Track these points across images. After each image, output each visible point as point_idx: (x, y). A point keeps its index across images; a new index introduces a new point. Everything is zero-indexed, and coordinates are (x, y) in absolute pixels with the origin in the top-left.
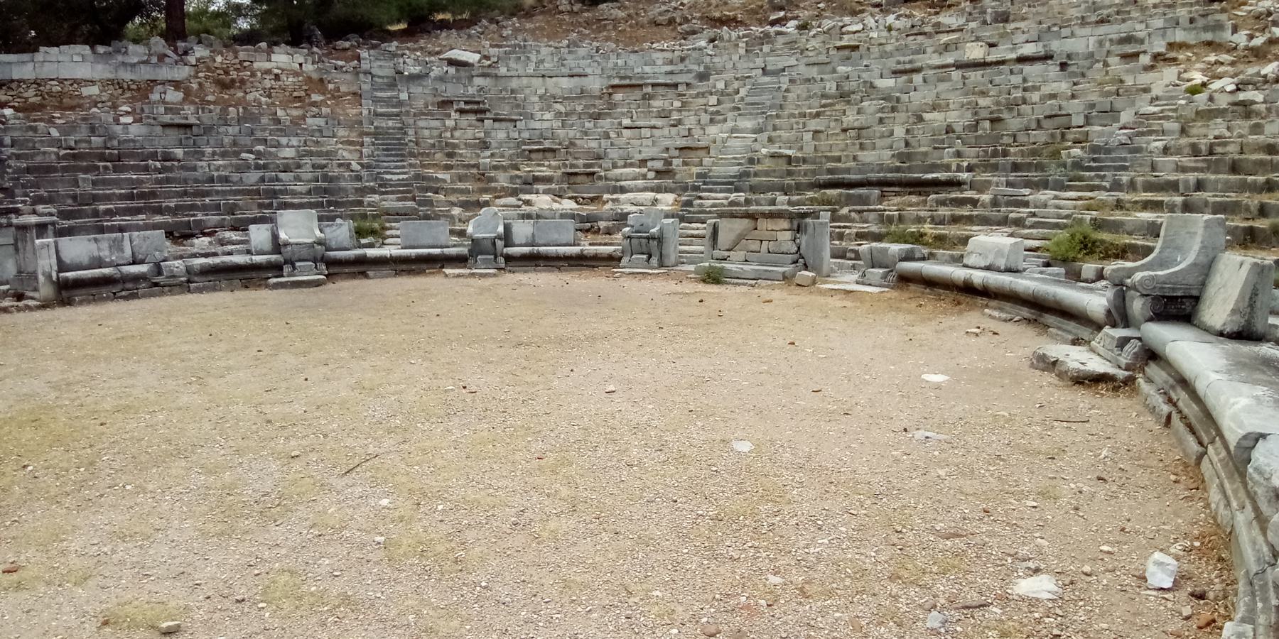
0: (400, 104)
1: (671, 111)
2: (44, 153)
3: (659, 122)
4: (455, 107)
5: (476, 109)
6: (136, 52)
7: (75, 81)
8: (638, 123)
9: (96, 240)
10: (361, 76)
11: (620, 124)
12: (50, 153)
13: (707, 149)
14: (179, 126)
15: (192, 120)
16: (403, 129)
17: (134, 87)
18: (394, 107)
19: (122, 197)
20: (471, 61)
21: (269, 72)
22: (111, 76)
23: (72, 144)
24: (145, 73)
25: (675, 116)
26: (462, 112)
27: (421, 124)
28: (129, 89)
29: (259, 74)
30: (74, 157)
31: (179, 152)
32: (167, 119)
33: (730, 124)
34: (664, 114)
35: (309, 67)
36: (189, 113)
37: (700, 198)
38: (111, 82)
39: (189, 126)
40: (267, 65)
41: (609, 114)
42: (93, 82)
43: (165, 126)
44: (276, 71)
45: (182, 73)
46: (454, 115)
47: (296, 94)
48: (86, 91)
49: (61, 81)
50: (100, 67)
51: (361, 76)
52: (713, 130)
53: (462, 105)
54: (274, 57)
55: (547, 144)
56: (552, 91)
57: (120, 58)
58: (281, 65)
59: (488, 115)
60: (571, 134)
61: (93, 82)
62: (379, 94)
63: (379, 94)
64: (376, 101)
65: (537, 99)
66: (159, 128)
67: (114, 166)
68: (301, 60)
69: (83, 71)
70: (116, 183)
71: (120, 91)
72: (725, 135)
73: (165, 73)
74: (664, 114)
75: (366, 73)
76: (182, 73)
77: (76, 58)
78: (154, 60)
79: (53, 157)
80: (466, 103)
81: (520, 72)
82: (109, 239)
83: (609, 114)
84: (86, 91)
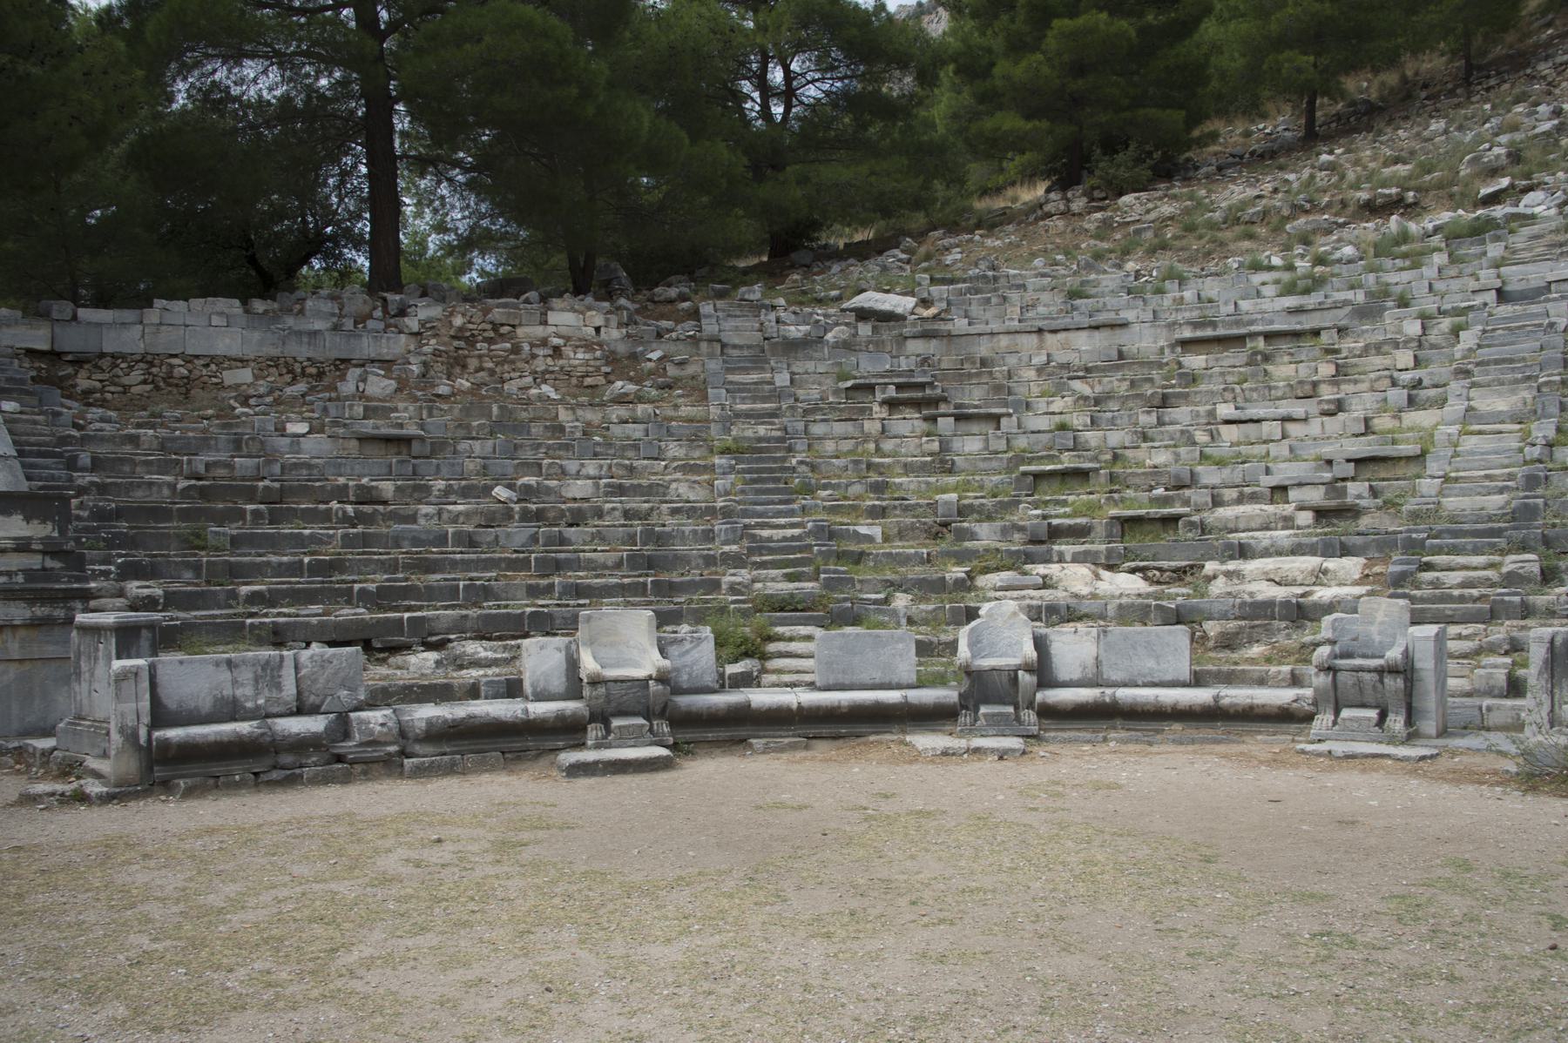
0: (777, 395)
1: (1315, 385)
2: (151, 484)
3: (1298, 409)
4: (879, 396)
5: (917, 397)
7: (213, 358)
8: (1253, 412)
9: (230, 664)
10: (704, 345)
11: (1212, 413)
12: (160, 485)
13: (1420, 458)
14: (388, 440)
15: (412, 430)
16: (785, 442)
17: (313, 371)
18: (765, 399)
19: (280, 570)
20: (899, 310)
21: (544, 342)
22: (274, 352)
23: (201, 469)
24: (333, 347)
25: (1327, 393)
26: (892, 404)
27: (818, 429)
28: (303, 374)
29: (526, 347)
30: (204, 493)
31: (387, 487)
32: (368, 426)
33: (1455, 407)
34: (1310, 391)
35: (613, 334)
36: (406, 418)
38: (274, 362)
39: (406, 441)
40: (539, 331)
41: (1186, 396)
42: (243, 362)
43: (364, 439)
44: (556, 341)
45: (396, 345)
46: (879, 411)
47: (588, 381)
48: (232, 377)
49: (189, 359)
50: (257, 335)
51: (704, 345)
52: (1422, 418)
53: (892, 392)
54: (553, 317)
55: (1067, 461)
56: (1061, 357)
57: (290, 321)
58: (563, 330)
59: (943, 408)
60: (1115, 438)
61: (243, 362)
62: (731, 377)
63: (731, 377)
64: (734, 390)
65: (1032, 374)
66: (354, 443)
67: (271, 511)
68: (599, 321)
69: (228, 342)
70: (274, 543)
71: (288, 378)
72: (1454, 429)
73: (367, 347)
74: (1310, 391)
75: (712, 340)
76: (396, 345)
77: (216, 320)
78: (349, 324)
79: (166, 492)
80: (899, 387)
81: (995, 326)
82: (255, 662)
83: (1186, 396)
84: (232, 377)
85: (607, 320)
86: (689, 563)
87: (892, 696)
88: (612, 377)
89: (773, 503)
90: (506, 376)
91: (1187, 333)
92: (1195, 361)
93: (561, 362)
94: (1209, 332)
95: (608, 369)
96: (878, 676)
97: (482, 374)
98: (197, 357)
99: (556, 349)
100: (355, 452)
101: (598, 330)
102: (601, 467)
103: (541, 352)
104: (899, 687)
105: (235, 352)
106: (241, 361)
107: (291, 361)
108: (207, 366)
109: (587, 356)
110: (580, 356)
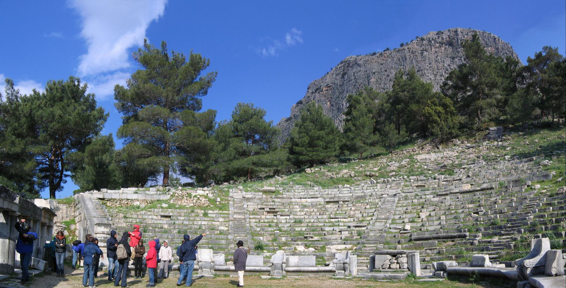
6: (152, 191)
14: (166, 217)
22: (144, 199)
24: (156, 198)
31: (166, 226)
32: (162, 214)
37: (365, 247)
43: (162, 216)
53: (268, 210)
57: (147, 192)
73: (163, 198)
80: (270, 209)
87: (257, 268)
91: (328, 200)
92: (328, 206)
94: (332, 200)
96: (255, 264)
104: (259, 266)
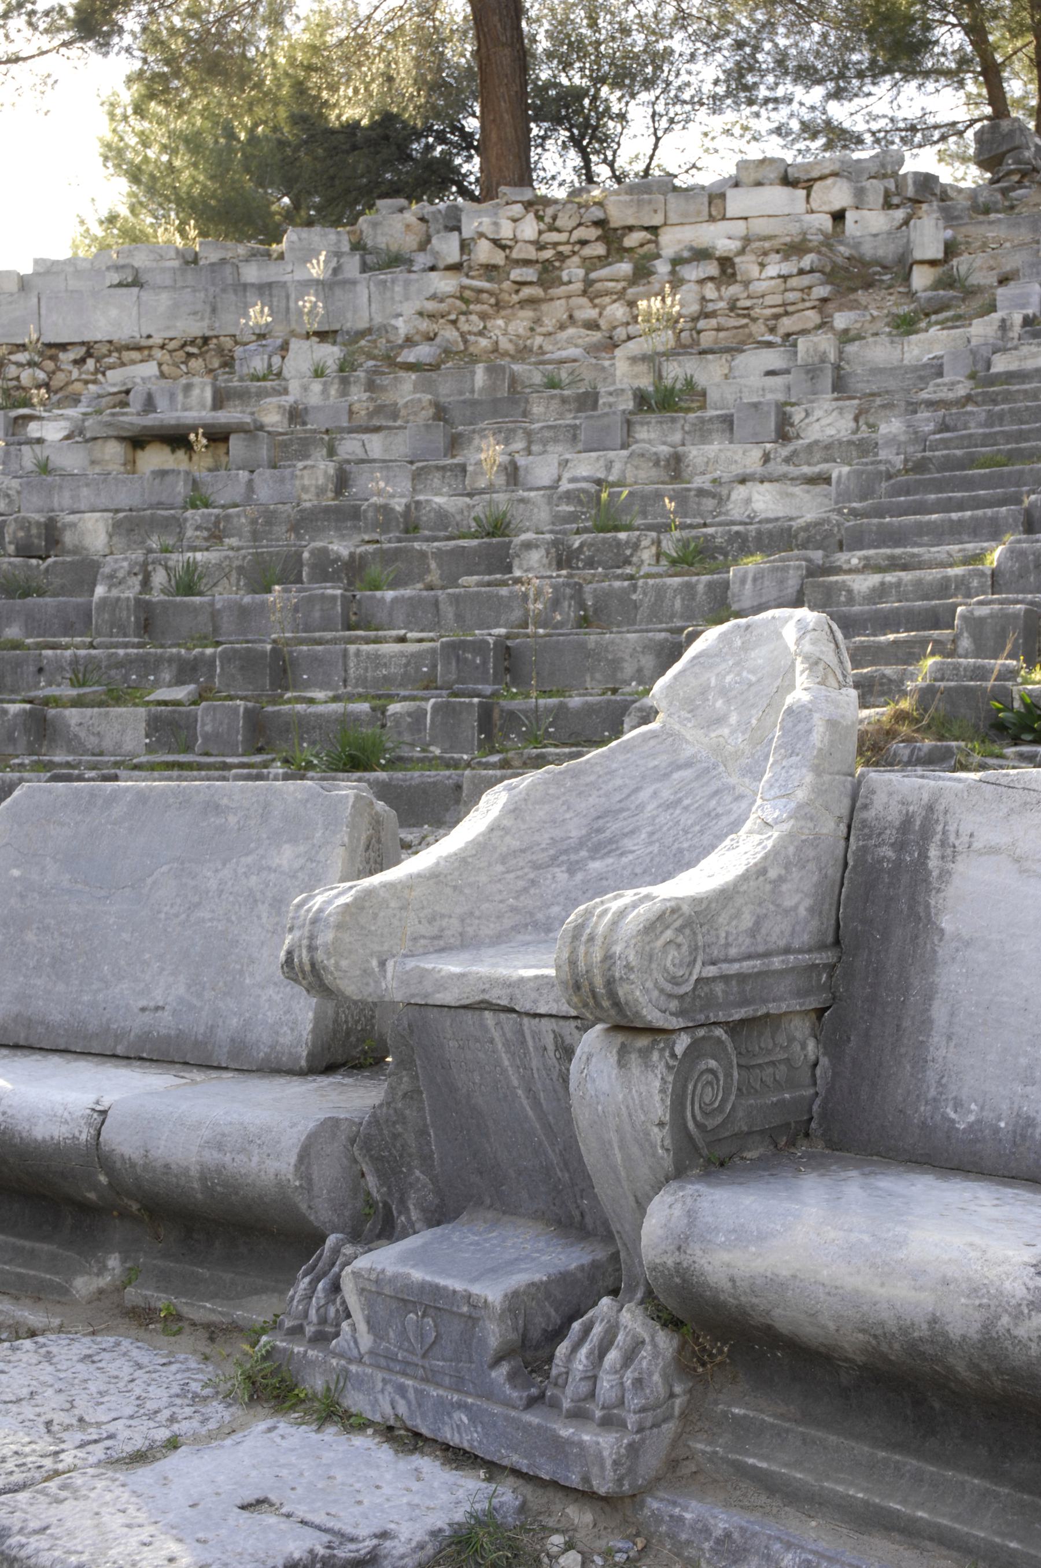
7: (89, 349)
21: (701, 255)
22: (196, 328)
47: (787, 324)
58: (760, 227)
66: (114, 451)
85: (860, 193)
86: (615, 664)
88: (831, 306)
89: (961, 506)
90: (620, 333)
93: (734, 290)
95: (822, 291)
97: (571, 331)
98: (63, 347)
99: (726, 263)
100: (115, 468)
101: (839, 217)
102: (609, 466)
103: (692, 273)
105: (126, 330)
106: (139, 348)
107: (228, 343)
108: (79, 362)
109: (786, 268)
110: (772, 271)
